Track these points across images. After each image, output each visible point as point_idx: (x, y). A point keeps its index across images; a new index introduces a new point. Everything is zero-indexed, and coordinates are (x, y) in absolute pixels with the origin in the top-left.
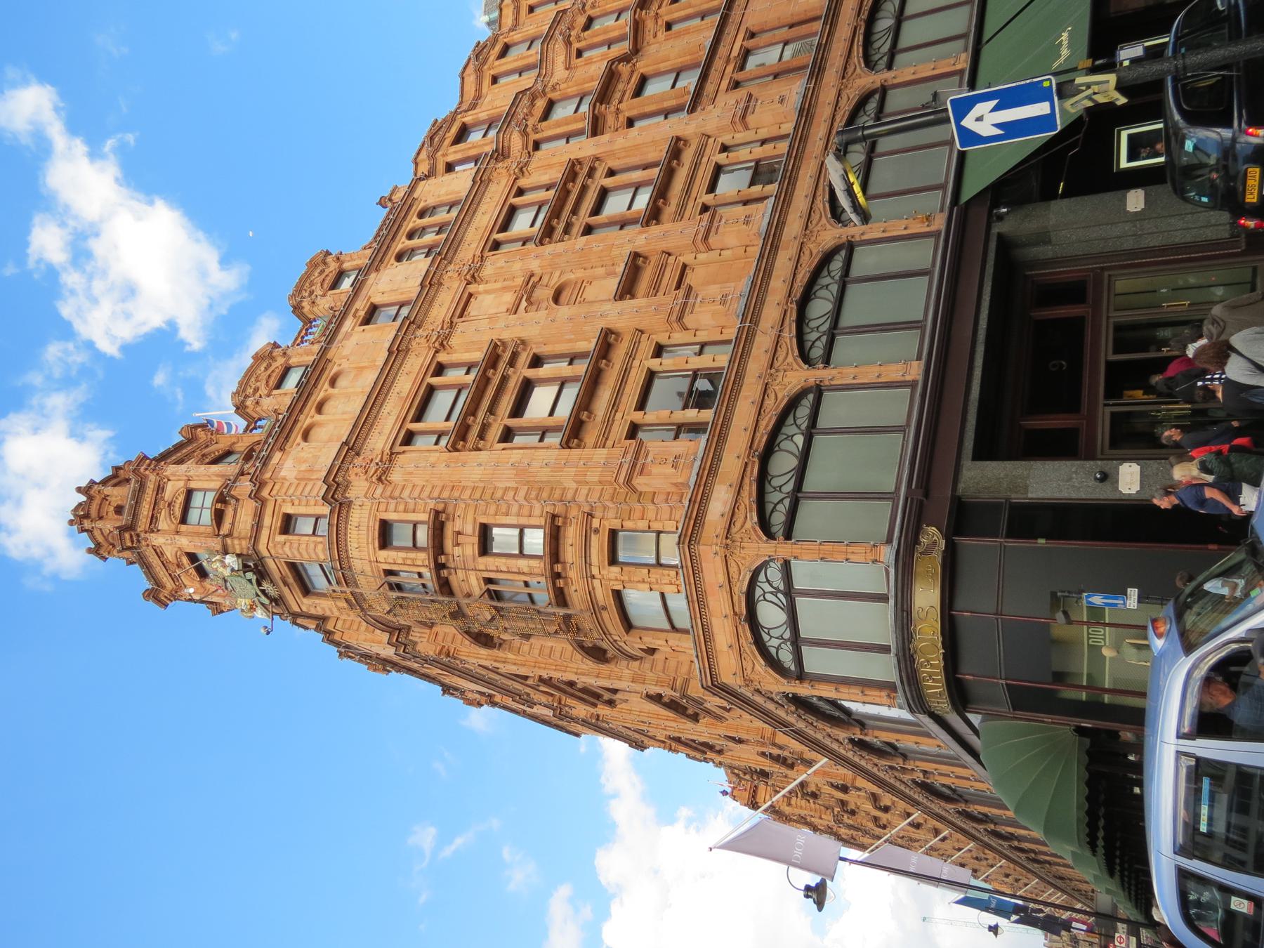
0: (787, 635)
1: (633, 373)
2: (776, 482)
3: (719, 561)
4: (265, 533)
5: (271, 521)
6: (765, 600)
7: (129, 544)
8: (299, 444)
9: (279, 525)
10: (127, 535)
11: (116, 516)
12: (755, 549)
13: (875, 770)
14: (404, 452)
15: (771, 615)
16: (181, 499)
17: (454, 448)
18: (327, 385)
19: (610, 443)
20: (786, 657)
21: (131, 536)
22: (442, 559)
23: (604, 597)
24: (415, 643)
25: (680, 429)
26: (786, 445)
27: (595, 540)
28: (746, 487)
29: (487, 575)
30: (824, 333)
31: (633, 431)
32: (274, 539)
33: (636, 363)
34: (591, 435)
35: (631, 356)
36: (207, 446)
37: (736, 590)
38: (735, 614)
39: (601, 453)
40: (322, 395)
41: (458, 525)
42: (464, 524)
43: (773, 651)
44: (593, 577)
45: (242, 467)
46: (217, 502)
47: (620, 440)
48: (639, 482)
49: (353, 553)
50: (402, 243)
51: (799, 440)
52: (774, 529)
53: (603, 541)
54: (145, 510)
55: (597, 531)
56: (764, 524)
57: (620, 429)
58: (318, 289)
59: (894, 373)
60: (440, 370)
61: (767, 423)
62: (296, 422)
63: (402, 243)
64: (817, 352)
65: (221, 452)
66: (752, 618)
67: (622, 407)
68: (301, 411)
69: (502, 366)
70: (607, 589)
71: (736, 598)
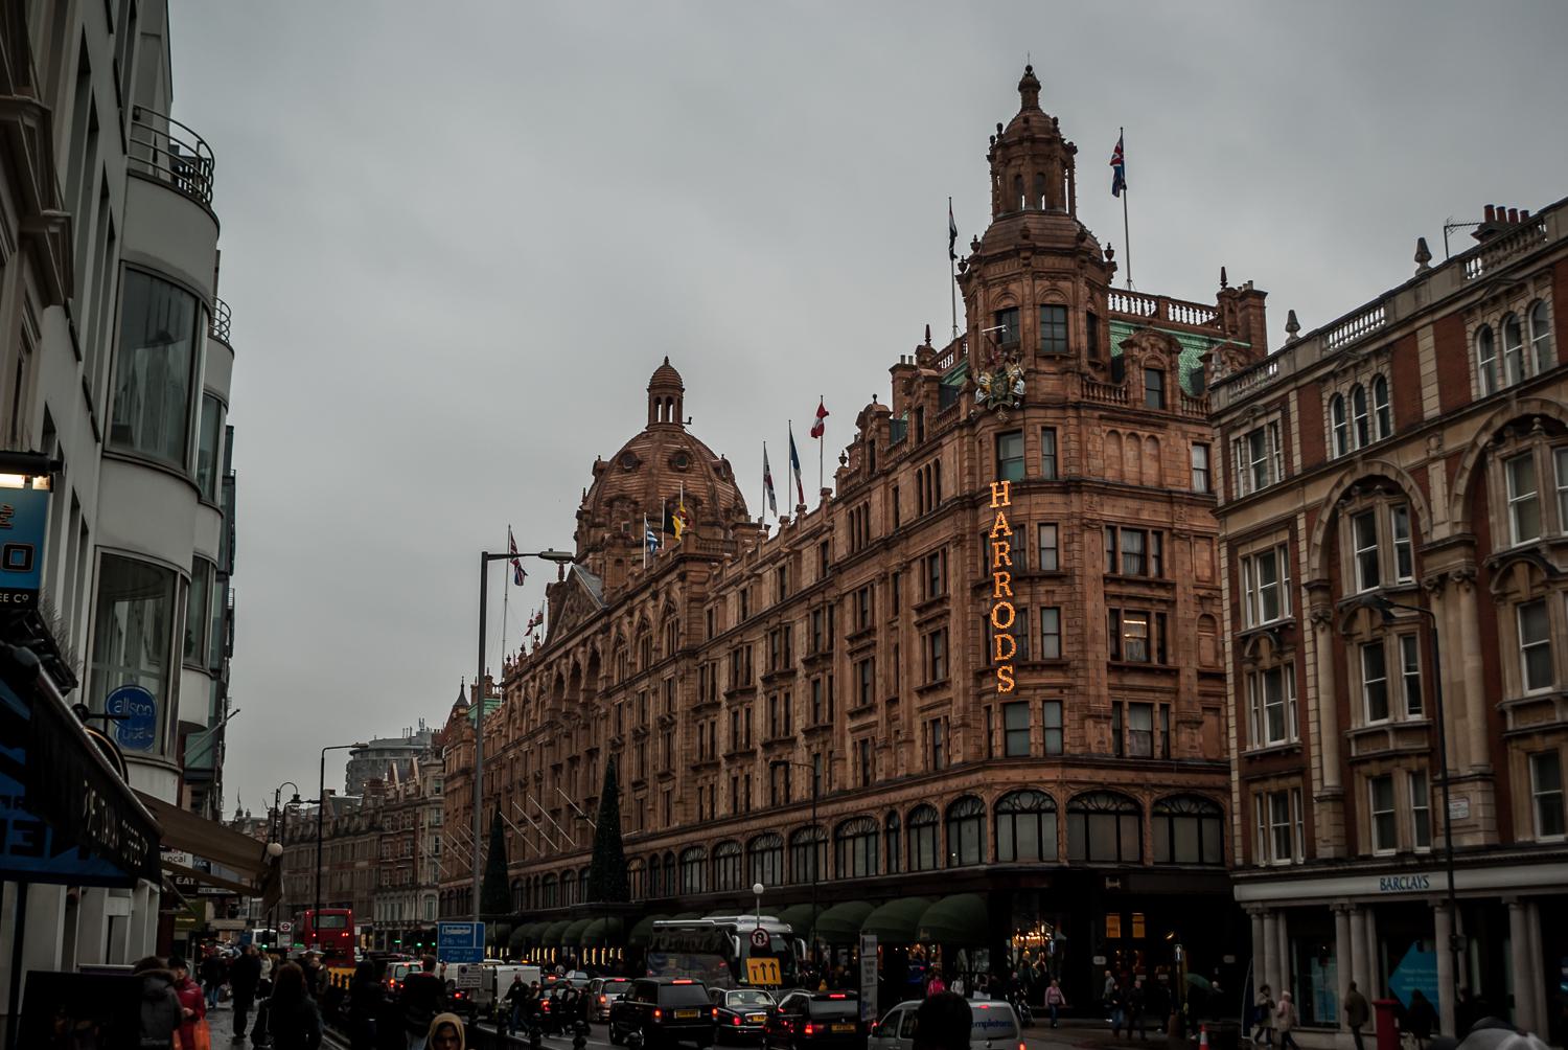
1: (1151, 694)
4: (1041, 413)
5: (1050, 416)
12: (1061, 797)
15: (1026, 802)
18: (1147, 434)
20: (1005, 806)
27: (1056, 691)
29: (1029, 611)
33: (1157, 695)
34: (1114, 680)
39: (1105, 691)
40: (1139, 433)
41: (1058, 589)
42: (1060, 594)
44: (1035, 689)
48: (1089, 723)
49: (1036, 498)
54: (1050, 262)
56: (1074, 799)
57: (1119, 695)
59: (1149, 853)
62: (1122, 421)
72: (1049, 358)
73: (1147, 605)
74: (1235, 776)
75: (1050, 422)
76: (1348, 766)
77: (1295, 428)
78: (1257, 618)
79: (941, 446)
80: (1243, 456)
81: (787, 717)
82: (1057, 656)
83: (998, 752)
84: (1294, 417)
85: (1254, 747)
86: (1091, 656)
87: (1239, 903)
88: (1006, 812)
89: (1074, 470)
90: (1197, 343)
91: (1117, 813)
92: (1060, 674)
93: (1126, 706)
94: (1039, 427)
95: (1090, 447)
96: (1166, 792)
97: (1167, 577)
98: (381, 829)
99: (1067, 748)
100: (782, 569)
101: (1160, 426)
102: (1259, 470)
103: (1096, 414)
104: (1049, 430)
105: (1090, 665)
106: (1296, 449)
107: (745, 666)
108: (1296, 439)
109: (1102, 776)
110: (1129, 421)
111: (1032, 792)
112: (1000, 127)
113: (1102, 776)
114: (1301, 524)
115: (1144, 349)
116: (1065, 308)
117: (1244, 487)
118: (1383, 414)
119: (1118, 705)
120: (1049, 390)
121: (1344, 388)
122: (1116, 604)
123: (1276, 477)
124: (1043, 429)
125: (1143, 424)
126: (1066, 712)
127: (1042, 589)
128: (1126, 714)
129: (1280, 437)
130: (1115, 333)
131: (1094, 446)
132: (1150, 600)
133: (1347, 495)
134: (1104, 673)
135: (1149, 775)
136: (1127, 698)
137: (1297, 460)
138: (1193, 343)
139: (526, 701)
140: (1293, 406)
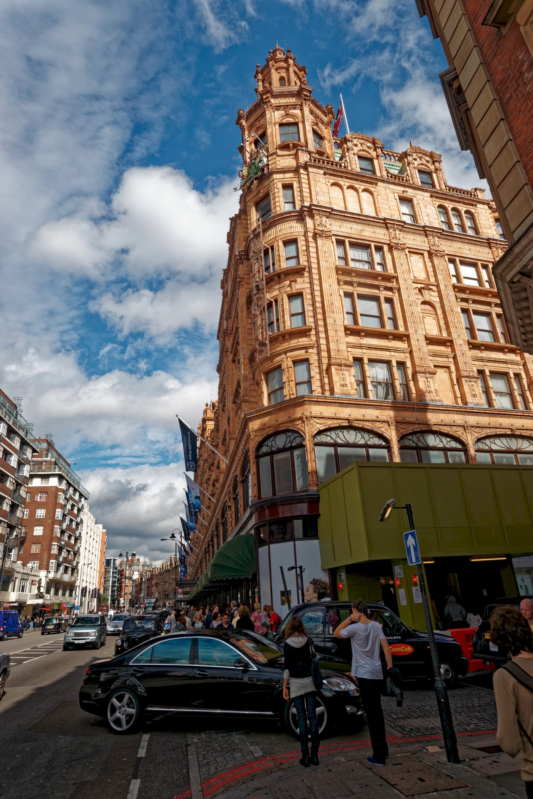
0: (273, 449)
1: (388, 353)
4: (281, 176)
6: (287, 437)
7: (264, 97)
8: (329, 182)
9: (287, 182)
11: (278, 78)
13: (227, 485)
14: (332, 242)
16: (291, 120)
17: (337, 269)
19: (349, 349)
20: (264, 449)
21: (268, 97)
22: (282, 276)
24: (242, 263)
25: (363, 382)
26: (359, 435)
27: (303, 351)
28: (336, 421)
30: (417, 444)
31: (358, 360)
32: (279, 182)
33: (393, 353)
34: (352, 339)
35: (396, 350)
36: (322, 123)
37: (289, 424)
38: (279, 425)
39: (343, 347)
43: (266, 443)
44: (286, 354)
45: (312, 153)
46: (293, 144)
47: (352, 354)
50: (449, 205)
51: (362, 442)
52: (318, 437)
53: (303, 356)
55: (306, 352)
56: (320, 432)
57: (358, 352)
58: (418, 163)
60: (379, 249)
61: (368, 425)
62: (341, 177)
63: (449, 205)
64: (407, 442)
65: (320, 133)
67: (369, 351)
68: (347, 178)
69: (383, 284)
70: (281, 361)
71: (285, 425)
73: (375, 292)
88: (265, 455)
93: (366, 361)
94: (280, 185)
101: (371, 183)
109: (346, 412)
113: (346, 412)
116: (296, 124)
122: (349, 289)
127: (287, 283)
128: (366, 367)
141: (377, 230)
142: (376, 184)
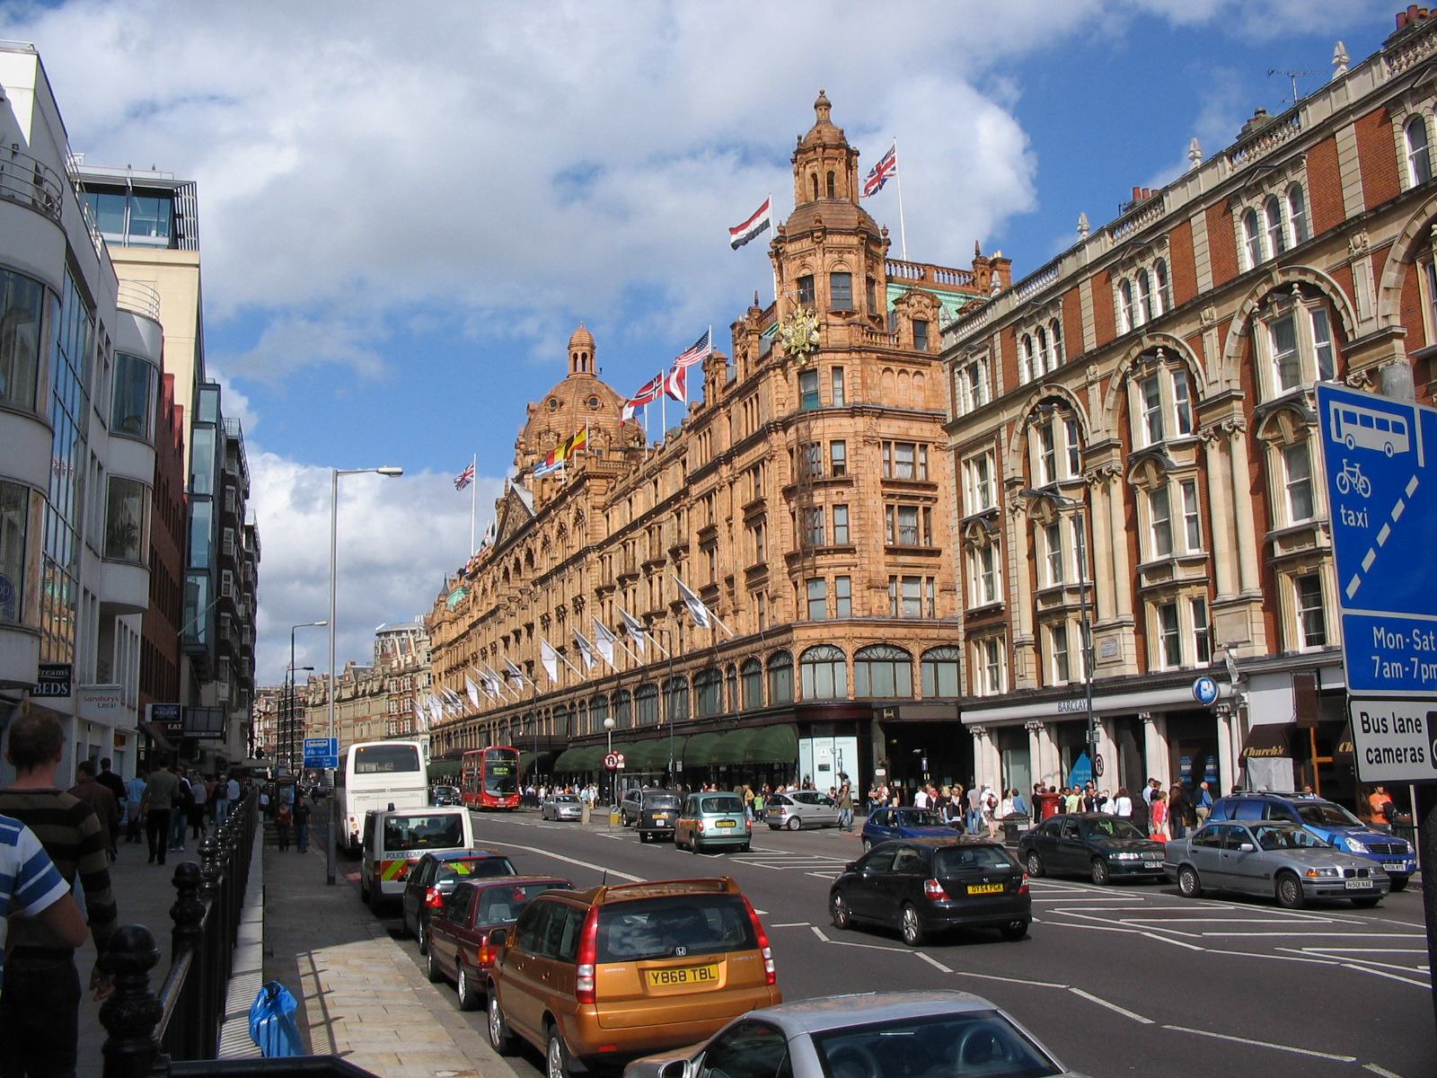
2: (874, 650)
3: (842, 634)
4: (832, 355)
5: (839, 358)
10: (820, 234)
12: (849, 649)
15: (824, 653)
18: (914, 370)
20: (807, 657)
23: (820, 572)
34: (890, 559)
39: (882, 568)
40: (908, 369)
42: (848, 494)
49: (828, 421)
51: (891, 657)
54: (835, 239)
56: (859, 650)
57: (894, 571)
59: (917, 690)
61: (897, 643)
66: (821, 646)
72: (837, 314)
74: (961, 628)
75: (838, 363)
76: (1038, 618)
77: (999, 361)
78: (974, 506)
79: (757, 385)
80: (964, 383)
81: (661, 595)
82: (845, 541)
83: (804, 616)
84: (998, 353)
85: (973, 606)
86: (872, 542)
87: (965, 725)
89: (858, 399)
90: (956, 299)
91: (894, 661)
92: (848, 556)
95: (869, 381)
96: (932, 643)
97: (932, 479)
98: (389, 691)
99: (854, 611)
100: (656, 483)
101: (924, 364)
102: (976, 393)
103: (874, 356)
104: (838, 370)
105: (871, 548)
106: (1000, 377)
107: (631, 557)
108: (999, 370)
110: (900, 361)
111: (826, 646)
112: (800, 138)
114: (1004, 435)
115: (913, 306)
116: (850, 274)
117: (966, 406)
118: (1058, 348)
119: (893, 578)
120: (838, 338)
121: (1031, 330)
122: (891, 501)
123: (986, 399)
124: (833, 368)
125: (909, 362)
126: (853, 585)
129: (989, 368)
130: (891, 293)
131: (873, 380)
132: (917, 498)
133: (1033, 412)
134: (882, 551)
135: (918, 631)
136: (900, 572)
137: (1001, 386)
138: (953, 299)
139: (484, 590)
140: (998, 344)
141: (925, 426)
142: (930, 365)
